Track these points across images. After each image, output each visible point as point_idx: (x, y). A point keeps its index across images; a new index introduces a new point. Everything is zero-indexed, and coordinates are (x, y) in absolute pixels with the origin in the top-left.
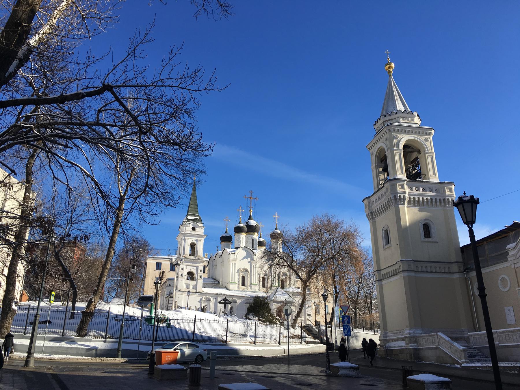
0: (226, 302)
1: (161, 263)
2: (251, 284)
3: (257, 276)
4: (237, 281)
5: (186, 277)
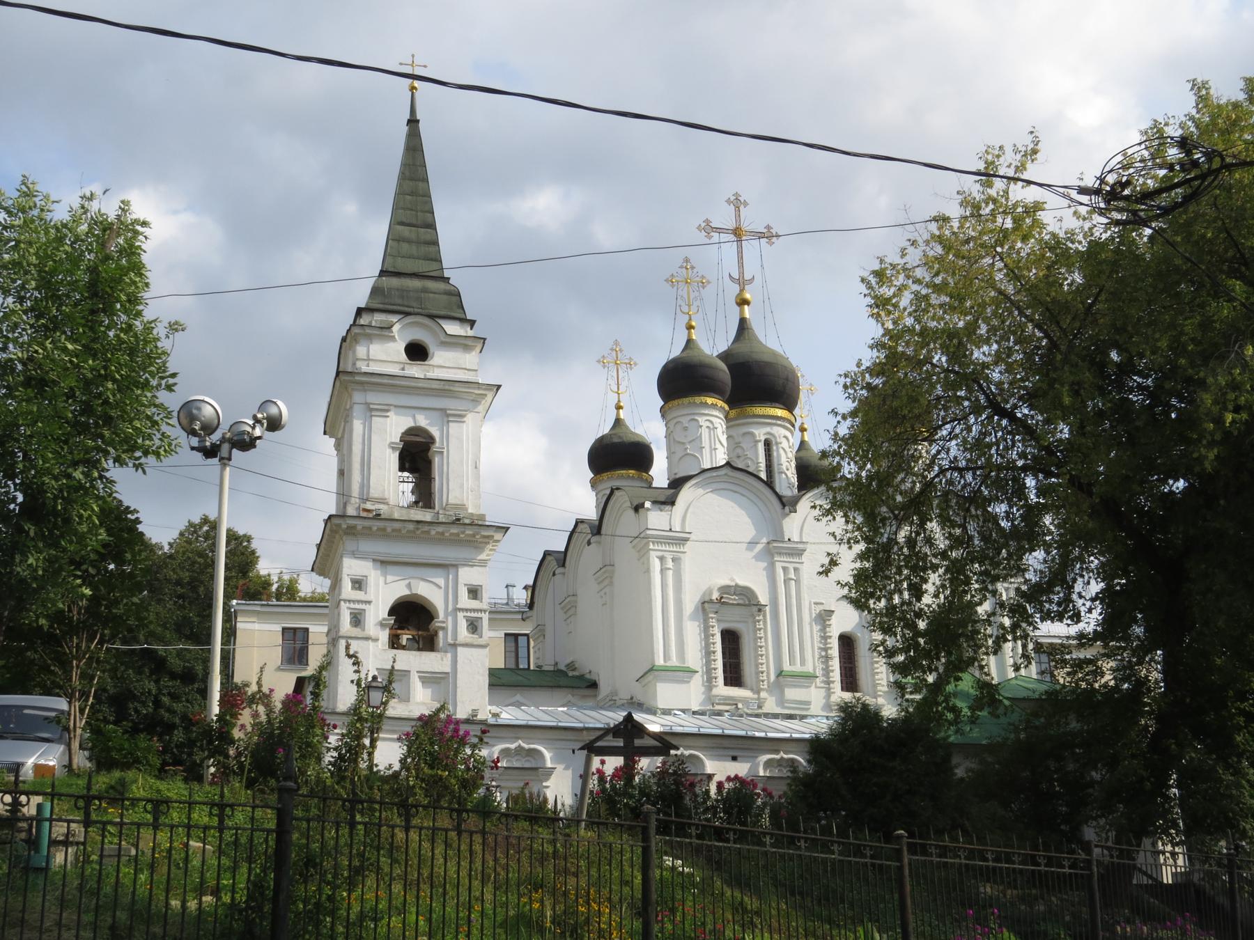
0: (638, 742)
1: (307, 630)
2: (780, 674)
3: (811, 633)
4: (694, 659)
5: (384, 636)
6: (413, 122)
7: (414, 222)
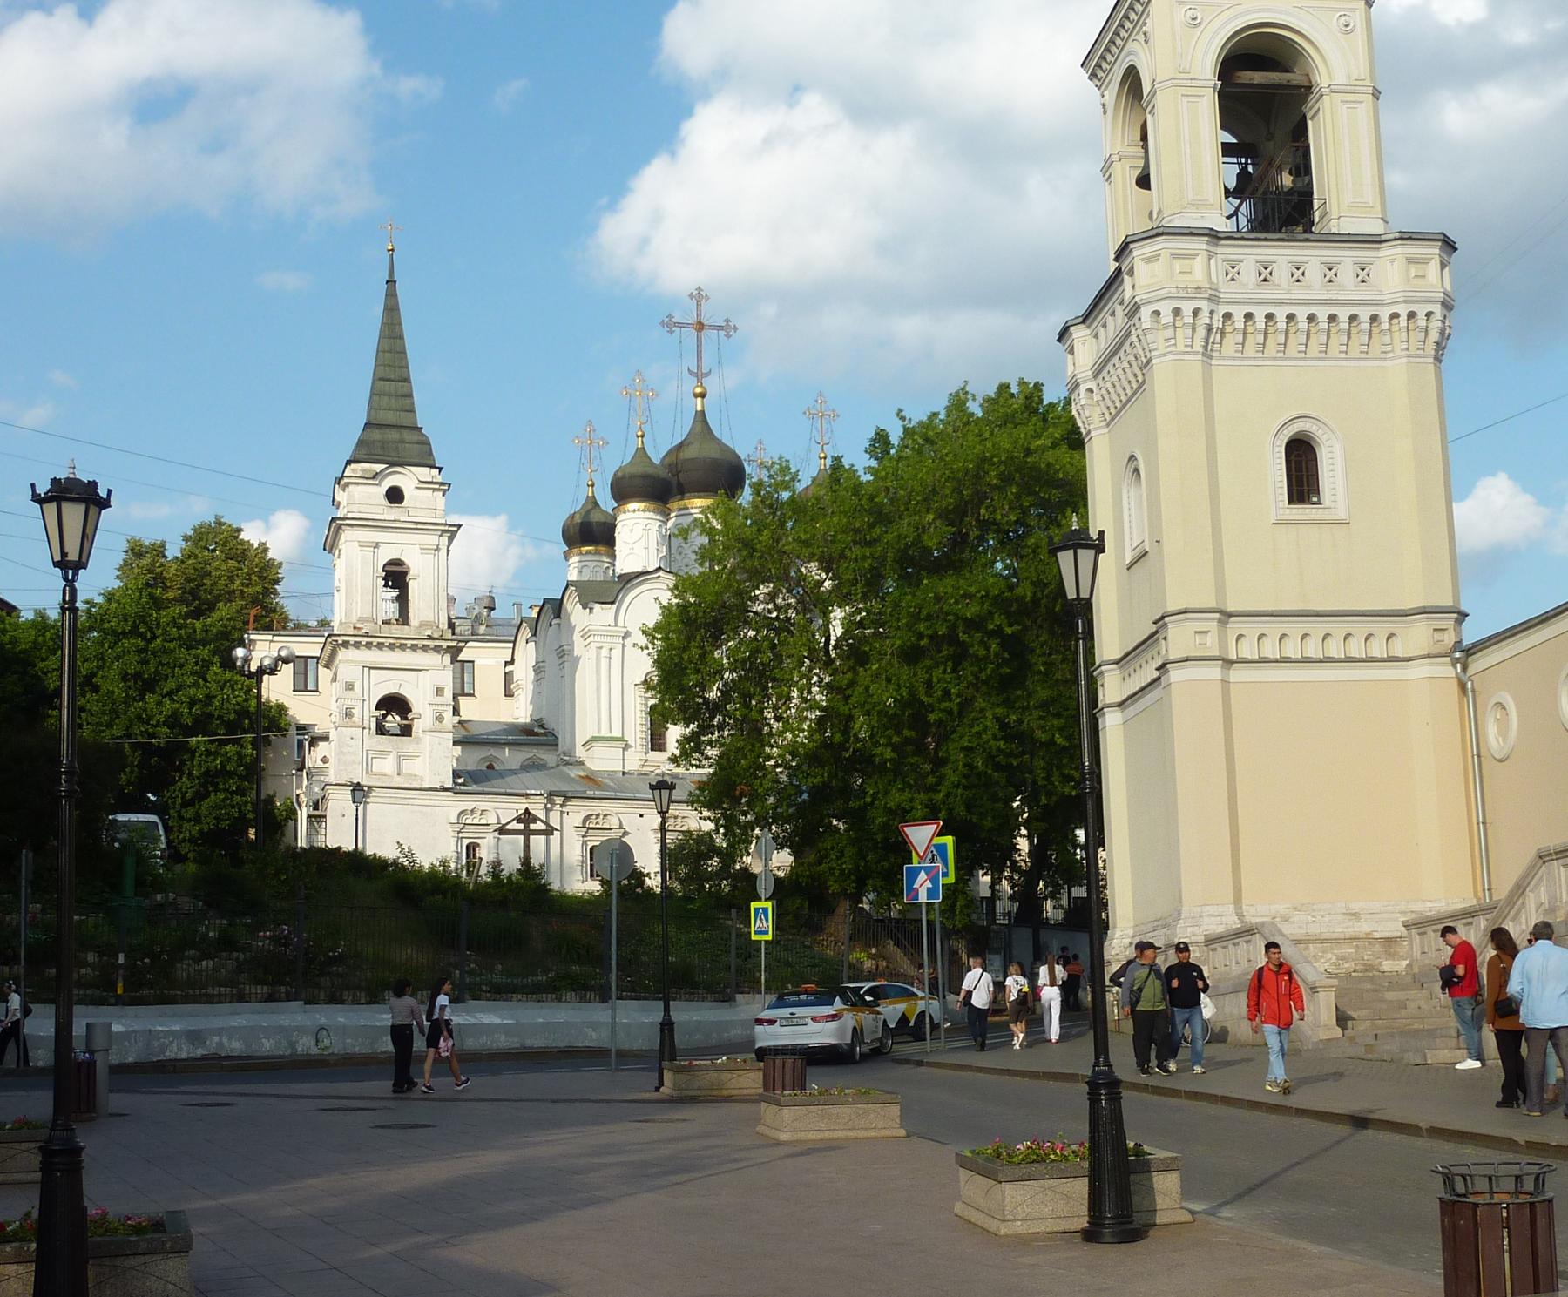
0: (532, 827)
6: (391, 282)
7: (392, 377)
